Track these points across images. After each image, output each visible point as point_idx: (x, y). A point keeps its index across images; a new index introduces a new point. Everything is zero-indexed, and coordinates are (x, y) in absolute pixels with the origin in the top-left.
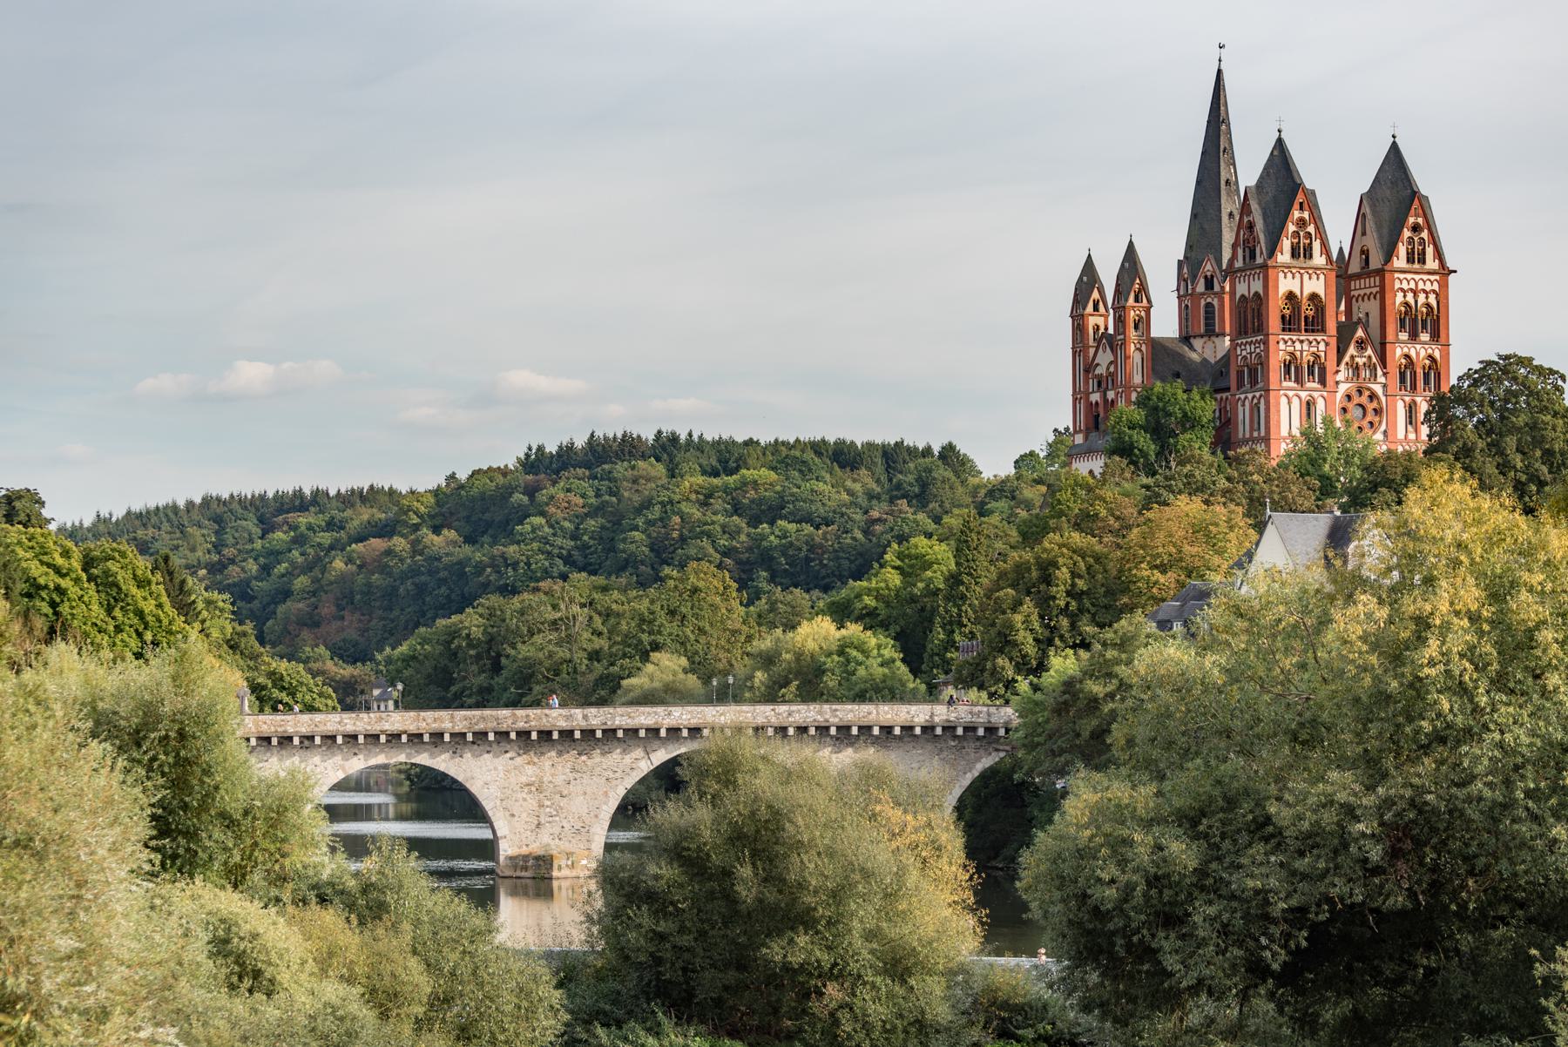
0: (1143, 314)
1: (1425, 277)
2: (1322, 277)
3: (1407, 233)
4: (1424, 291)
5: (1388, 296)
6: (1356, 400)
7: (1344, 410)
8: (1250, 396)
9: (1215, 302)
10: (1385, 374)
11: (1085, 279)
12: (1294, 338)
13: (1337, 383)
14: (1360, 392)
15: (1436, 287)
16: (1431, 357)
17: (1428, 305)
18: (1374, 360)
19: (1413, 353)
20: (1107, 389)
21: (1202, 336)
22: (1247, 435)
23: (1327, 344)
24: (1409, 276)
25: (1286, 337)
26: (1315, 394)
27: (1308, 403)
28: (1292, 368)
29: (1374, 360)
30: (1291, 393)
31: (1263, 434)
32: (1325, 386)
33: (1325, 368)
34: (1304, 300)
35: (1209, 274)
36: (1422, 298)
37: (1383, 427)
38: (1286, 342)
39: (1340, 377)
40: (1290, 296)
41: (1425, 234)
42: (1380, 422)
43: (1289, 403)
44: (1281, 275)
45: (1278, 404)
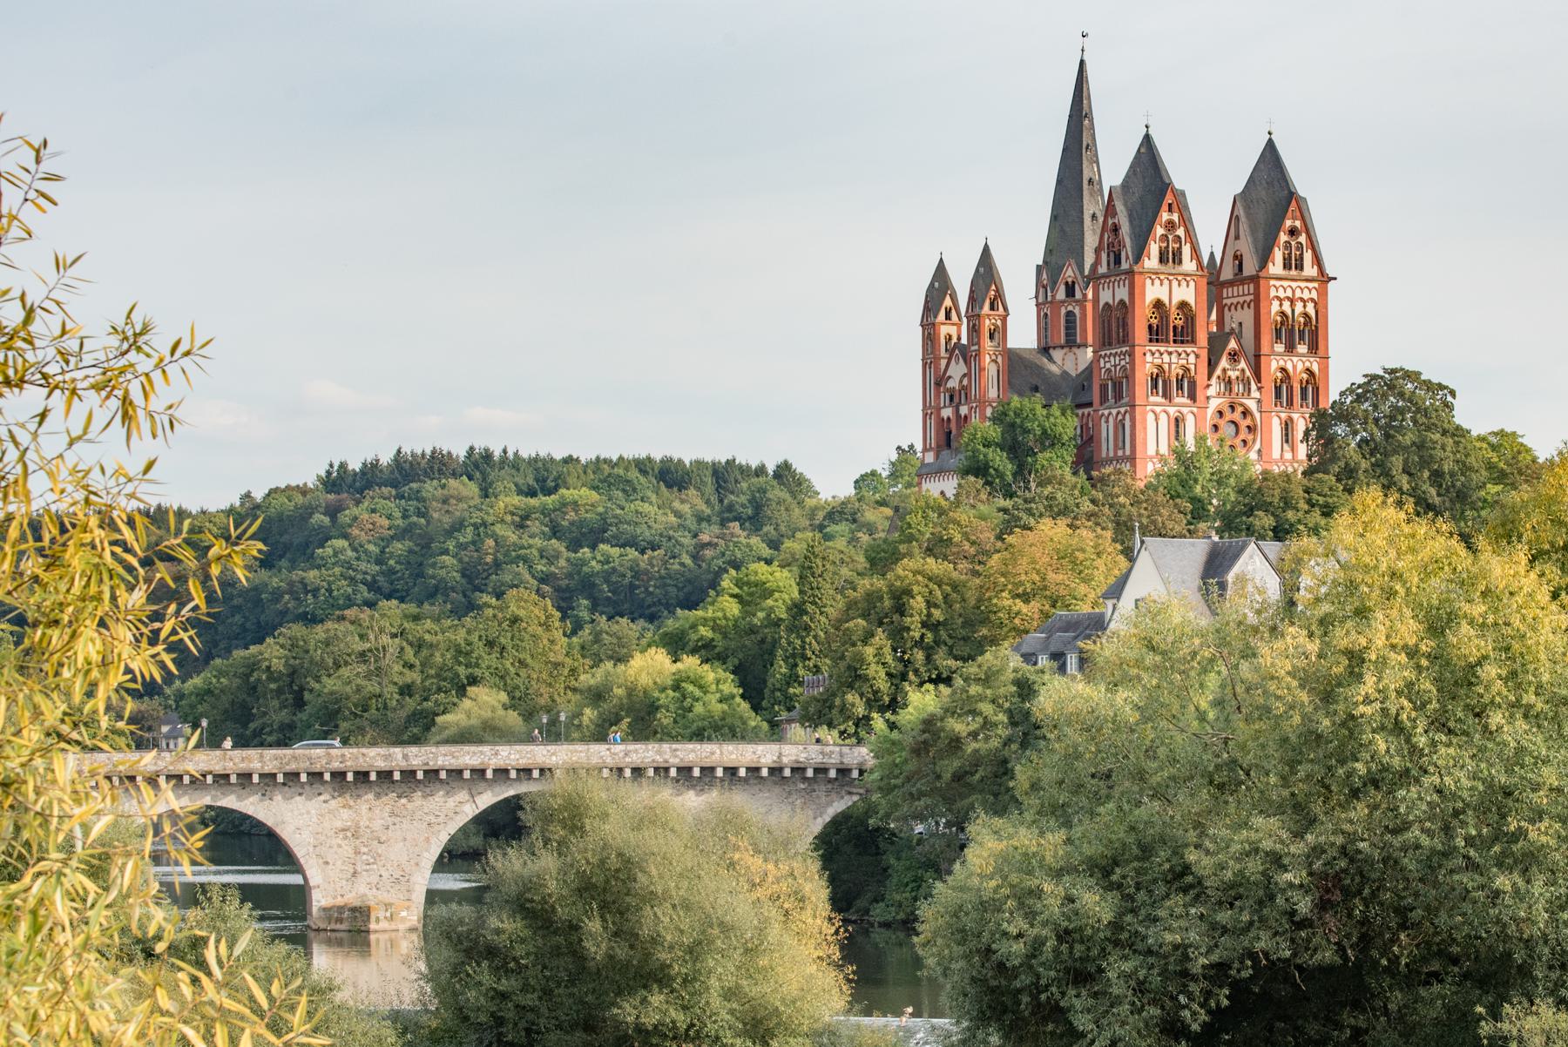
0: (999, 323)
1: (1303, 284)
2: (1192, 284)
3: (1283, 237)
4: (1302, 299)
5: (1263, 304)
6: (1228, 416)
7: (1216, 427)
8: (1114, 412)
9: (1077, 311)
10: (1259, 389)
11: (936, 284)
12: (1162, 349)
13: (1208, 398)
14: (1233, 408)
15: (1314, 295)
16: (1309, 371)
17: (1306, 315)
18: (1248, 373)
19: (1289, 367)
20: (960, 403)
21: (1062, 347)
22: (1111, 454)
23: (1197, 356)
24: (1285, 284)
25: (1154, 349)
26: (1185, 410)
27: (1177, 420)
28: (1158, 381)
30: (1158, 409)
31: (1128, 452)
32: (1195, 401)
33: (1195, 382)
34: (1173, 309)
35: (1070, 280)
36: (1299, 308)
37: (1257, 446)
38: (1153, 354)
39: (1212, 391)
40: (1158, 304)
41: (1303, 239)
42: (1254, 441)
44: (1148, 282)
45: (1145, 420)
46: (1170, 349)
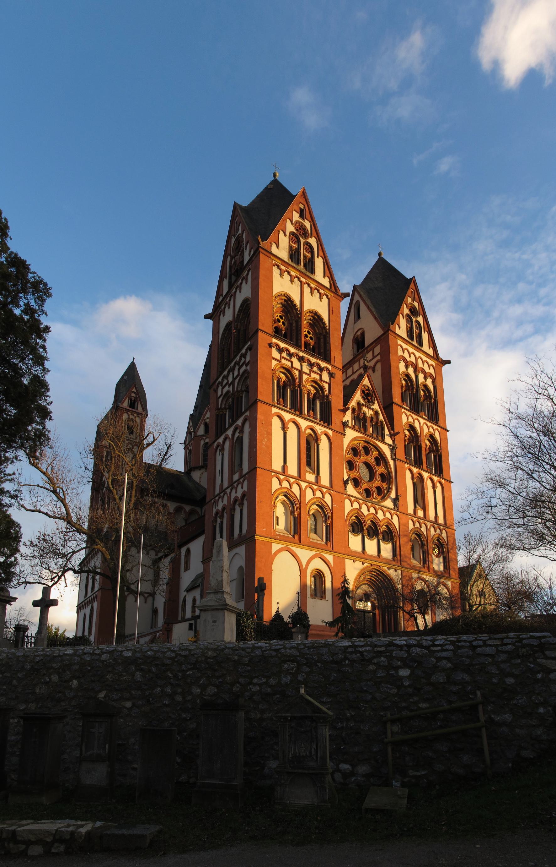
18: (381, 417)
19: (417, 425)
23: (331, 375)
29: (381, 417)
31: (245, 469)
37: (393, 495)
43: (284, 428)
46: (301, 354)
